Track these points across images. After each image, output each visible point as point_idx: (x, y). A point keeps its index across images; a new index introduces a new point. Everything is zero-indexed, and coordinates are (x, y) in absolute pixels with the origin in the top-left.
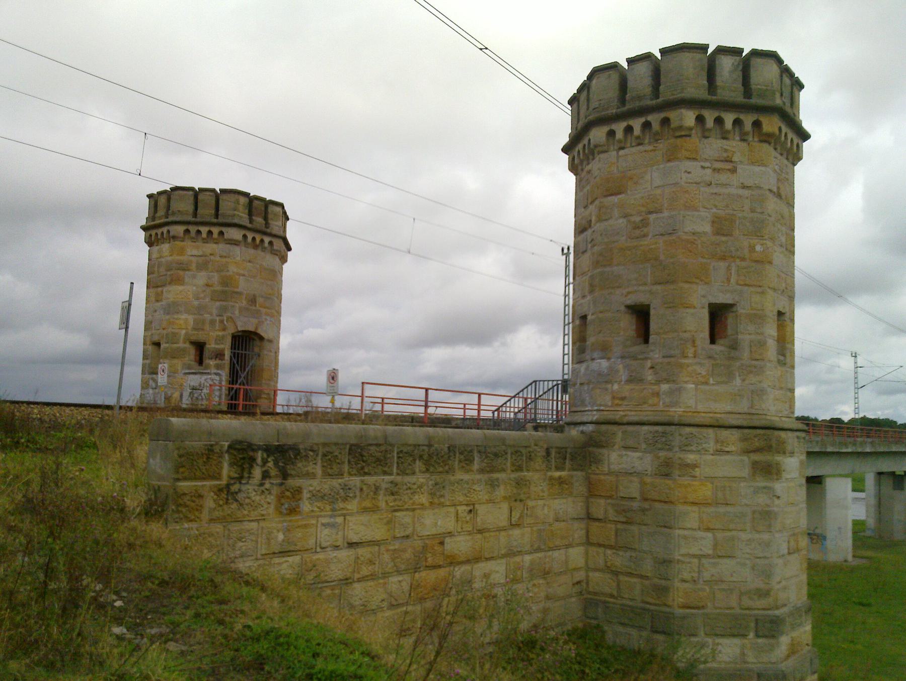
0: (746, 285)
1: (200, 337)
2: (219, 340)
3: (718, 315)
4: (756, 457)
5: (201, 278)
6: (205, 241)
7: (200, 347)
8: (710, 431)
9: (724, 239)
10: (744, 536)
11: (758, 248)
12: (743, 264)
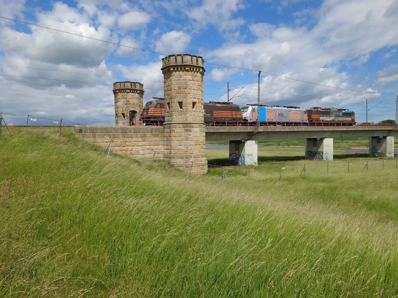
1: (124, 113)
3: (181, 104)
4: (185, 128)
7: (123, 115)
9: (180, 90)
10: (183, 142)
11: (186, 91)
12: (184, 94)
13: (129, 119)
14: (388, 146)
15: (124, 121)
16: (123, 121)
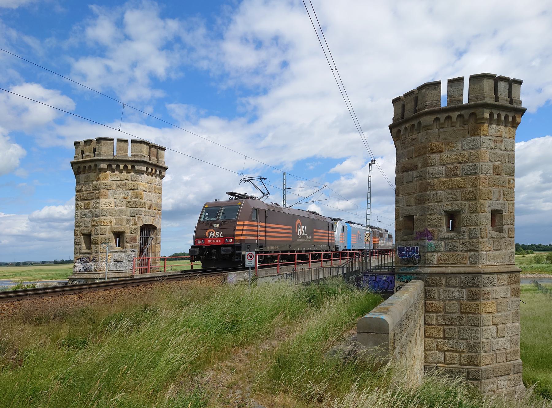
0: (507, 200)
1: (120, 229)
2: (132, 232)
5: (120, 194)
6: (121, 172)
7: (119, 236)
8: (496, 275)
9: (497, 177)
10: (508, 325)
12: (505, 190)
13: (137, 250)
15: (123, 255)
16: (117, 256)
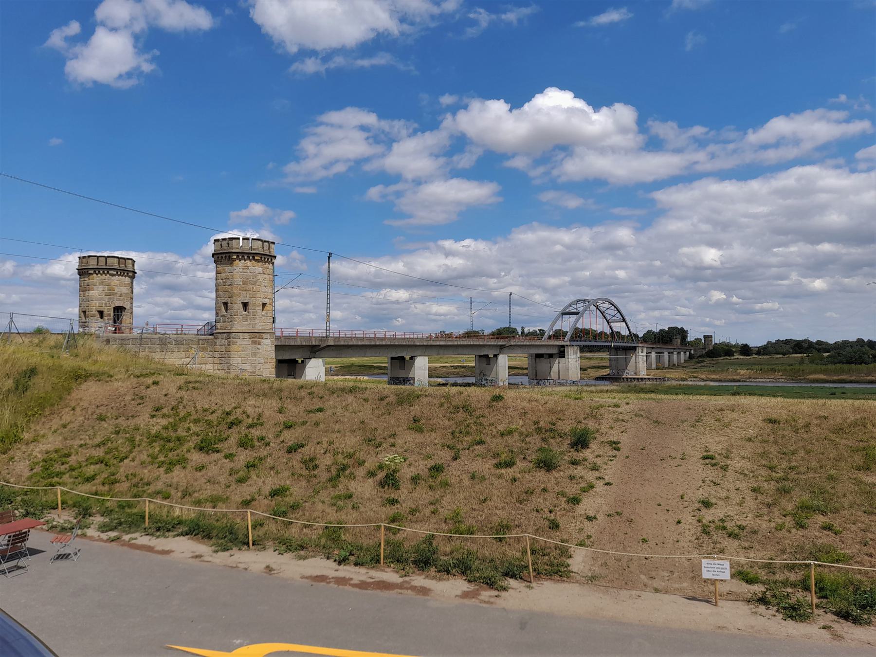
1: (101, 309)
2: (109, 311)
3: (245, 305)
5: (101, 288)
7: (101, 313)
14: (500, 369)
16: (100, 325)
